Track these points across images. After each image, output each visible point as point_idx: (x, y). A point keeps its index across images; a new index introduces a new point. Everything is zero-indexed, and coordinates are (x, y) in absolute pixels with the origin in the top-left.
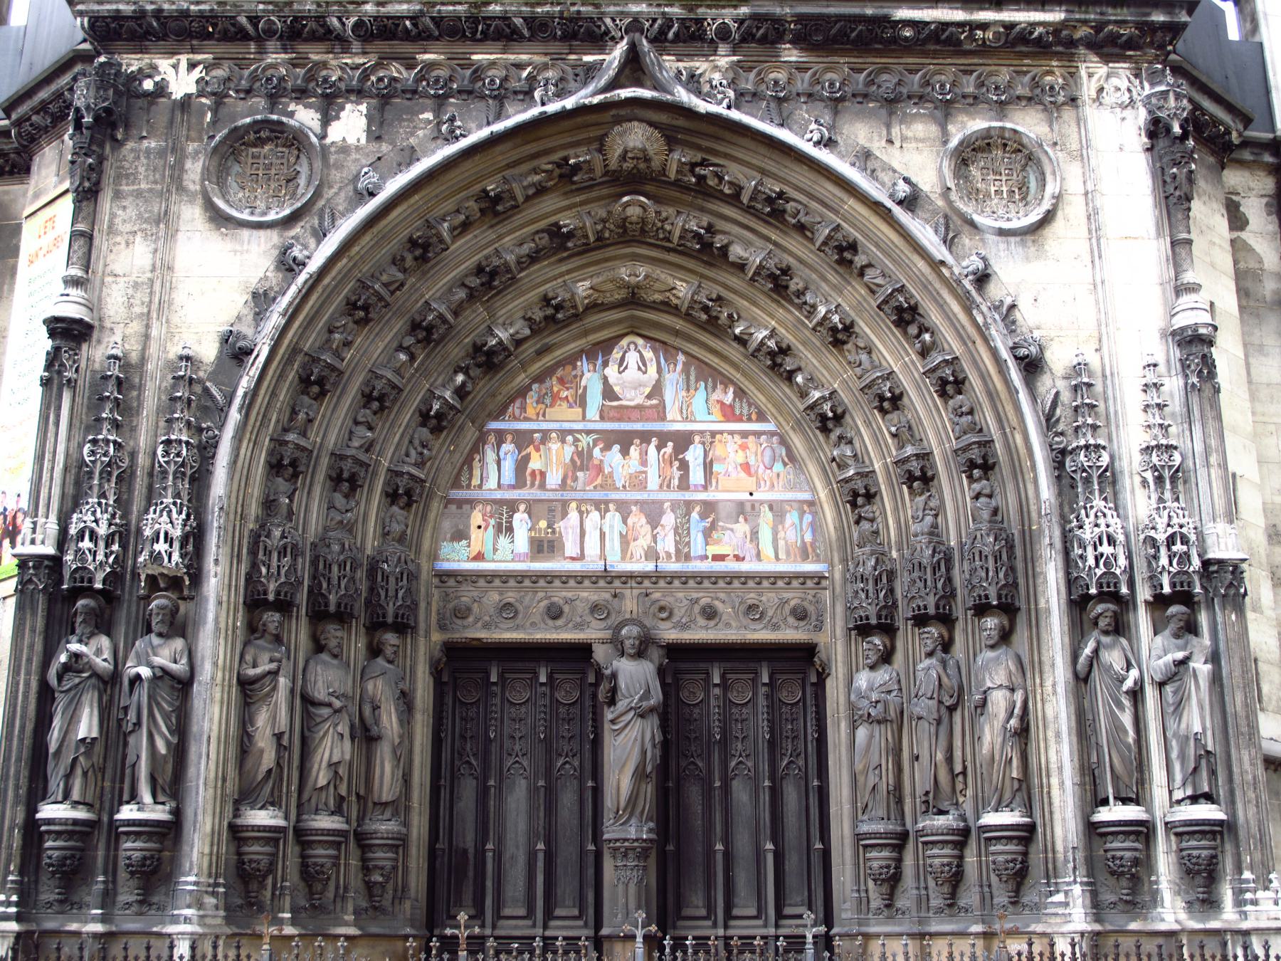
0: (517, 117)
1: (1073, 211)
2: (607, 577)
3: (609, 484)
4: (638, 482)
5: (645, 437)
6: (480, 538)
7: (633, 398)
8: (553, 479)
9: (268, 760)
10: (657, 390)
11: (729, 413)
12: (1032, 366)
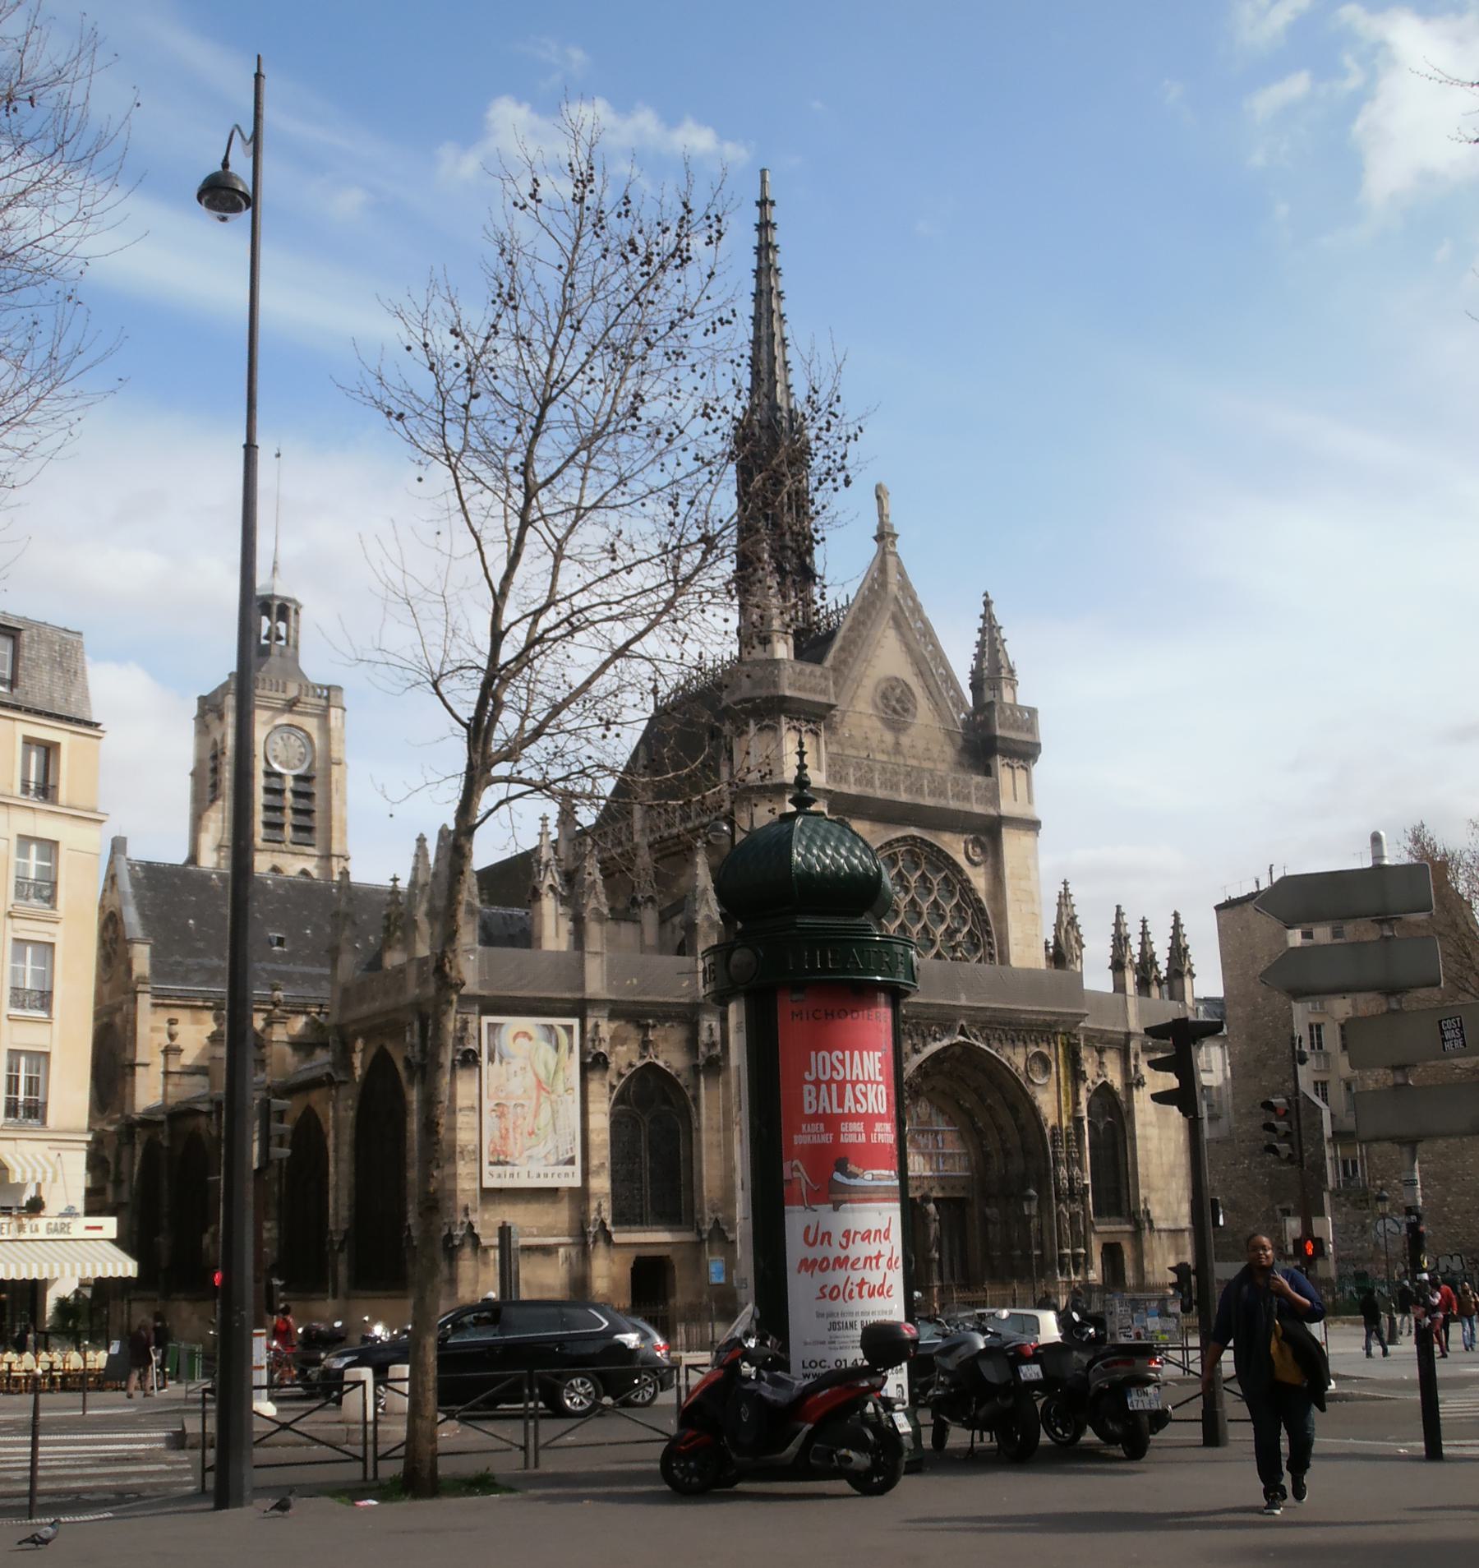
0: (933, 1047)
2: (920, 1177)
4: (926, 1146)
5: (928, 1131)
10: (930, 1116)
11: (948, 1125)
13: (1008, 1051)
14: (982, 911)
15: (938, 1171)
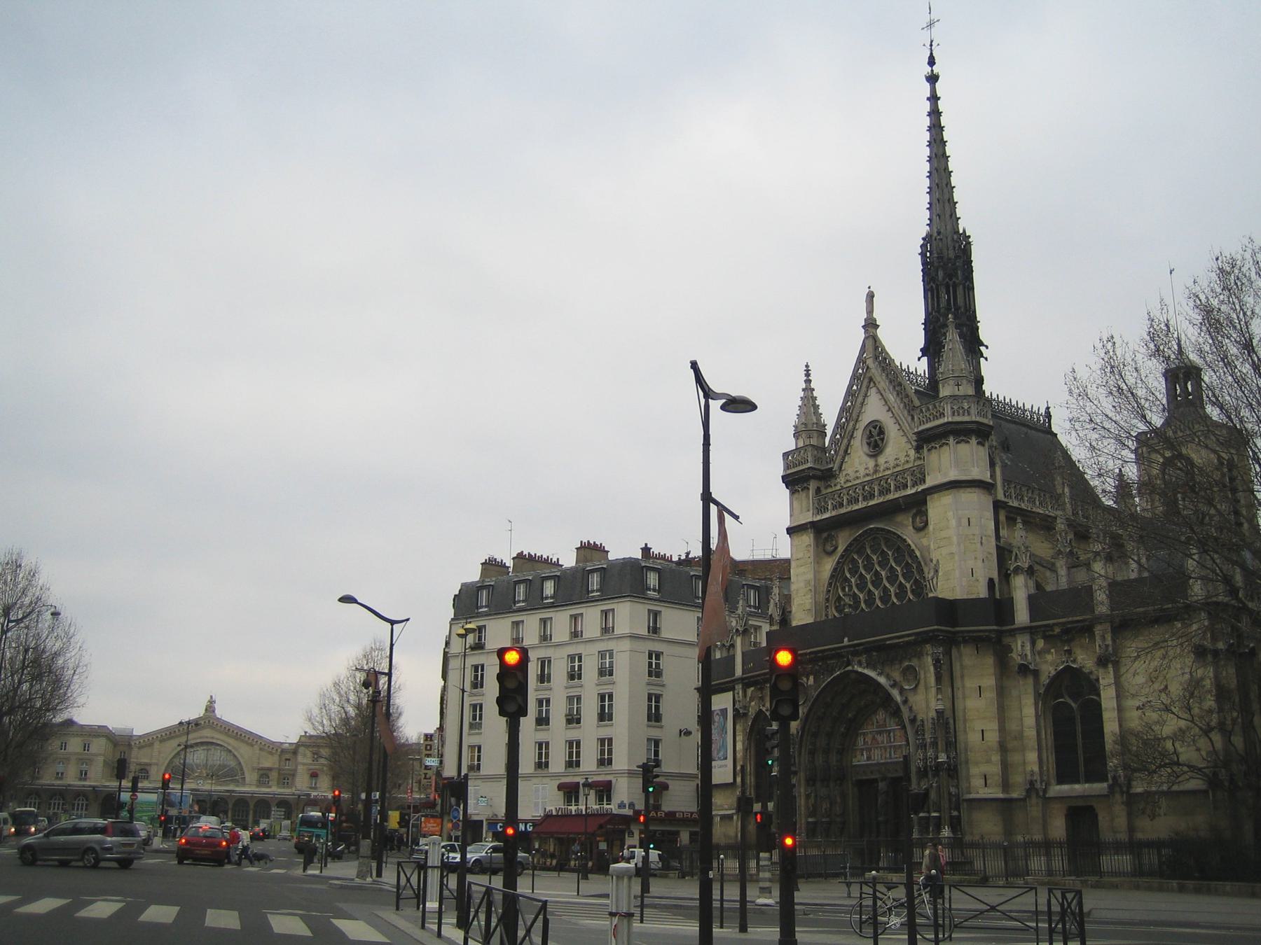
1: (922, 682)
2: (878, 764)
3: (878, 743)
4: (883, 742)
5: (883, 731)
6: (859, 757)
7: (881, 723)
8: (870, 743)
9: (811, 809)
12: (913, 721)
13: (887, 669)
14: (920, 562)
15: (891, 758)
